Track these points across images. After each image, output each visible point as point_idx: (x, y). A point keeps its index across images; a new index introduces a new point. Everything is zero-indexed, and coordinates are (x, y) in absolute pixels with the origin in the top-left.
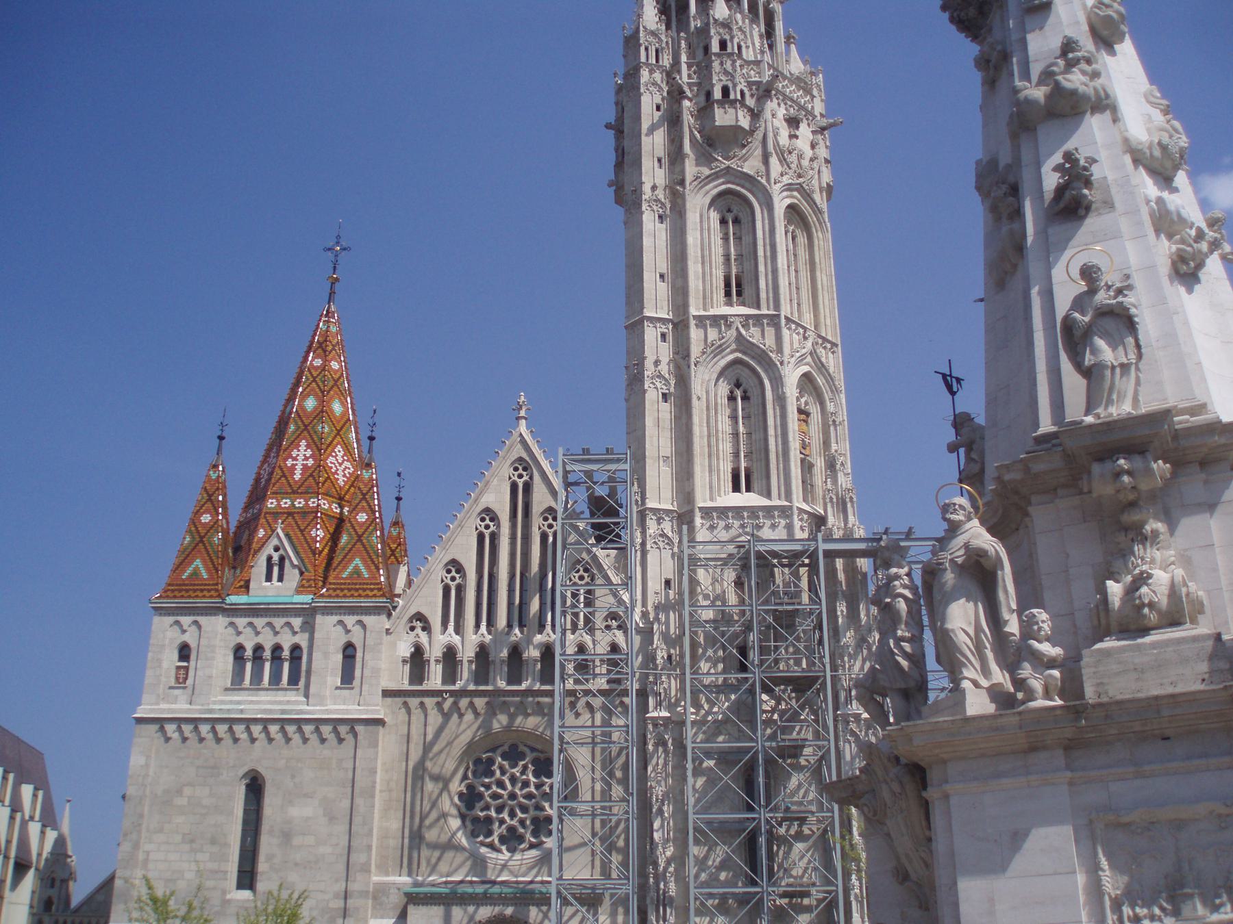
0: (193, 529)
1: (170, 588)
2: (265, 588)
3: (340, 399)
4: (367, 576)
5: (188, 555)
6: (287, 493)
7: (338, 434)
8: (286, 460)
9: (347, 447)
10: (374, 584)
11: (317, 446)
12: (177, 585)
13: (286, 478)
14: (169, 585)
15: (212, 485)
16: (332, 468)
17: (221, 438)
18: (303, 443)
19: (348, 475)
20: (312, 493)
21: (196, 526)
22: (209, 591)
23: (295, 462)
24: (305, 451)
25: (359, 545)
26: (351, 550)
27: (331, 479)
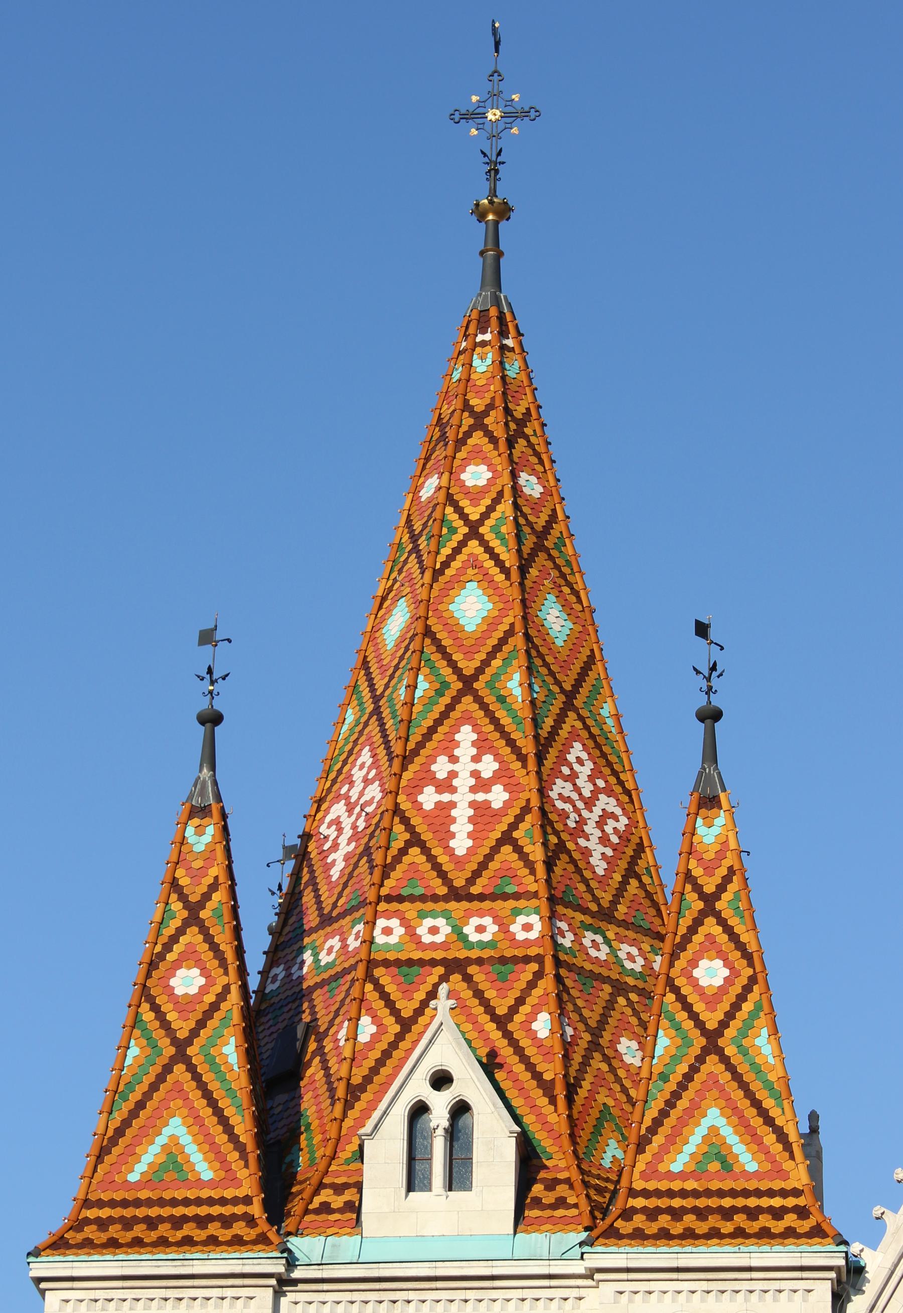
0: (148, 1016)
1: (91, 1214)
3: (560, 595)
4: (752, 1167)
5: (140, 1105)
6: (435, 898)
7: (569, 705)
8: (416, 788)
9: (598, 746)
10: (784, 1193)
12: (112, 1204)
13: (425, 850)
15: (196, 875)
16: (564, 815)
17: (211, 719)
18: (466, 735)
19: (615, 839)
20: (517, 896)
22: (227, 1222)
23: (446, 797)
24: (476, 759)
25: (712, 1064)
26: (688, 1077)
27: (568, 852)
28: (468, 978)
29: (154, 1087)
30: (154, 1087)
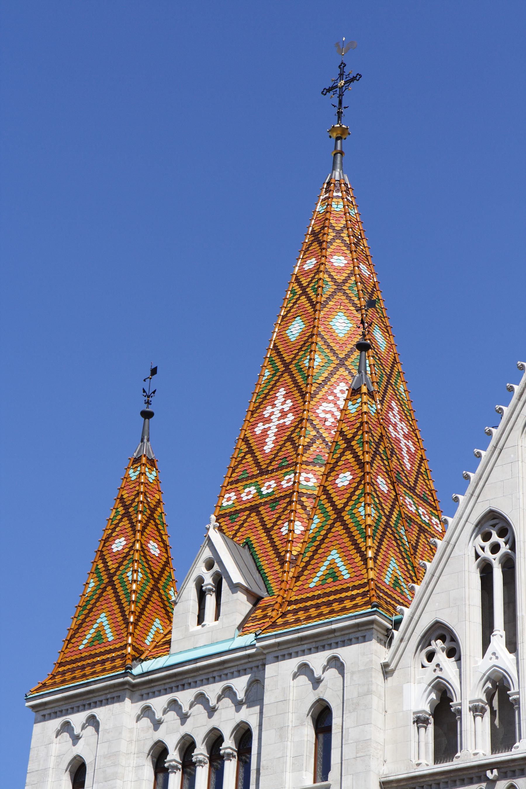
0: (101, 566)
1: (60, 669)
2: (193, 635)
5: (91, 610)
6: (253, 477)
8: (255, 425)
11: (300, 390)
14: (61, 664)
16: (326, 420)
17: (147, 415)
18: (282, 391)
21: (105, 562)
22: (113, 660)
23: (267, 426)
24: (283, 403)
25: (338, 528)
26: (325, 536)
28: (258, 513)
29: (98, 600)
30: (98, 600)
